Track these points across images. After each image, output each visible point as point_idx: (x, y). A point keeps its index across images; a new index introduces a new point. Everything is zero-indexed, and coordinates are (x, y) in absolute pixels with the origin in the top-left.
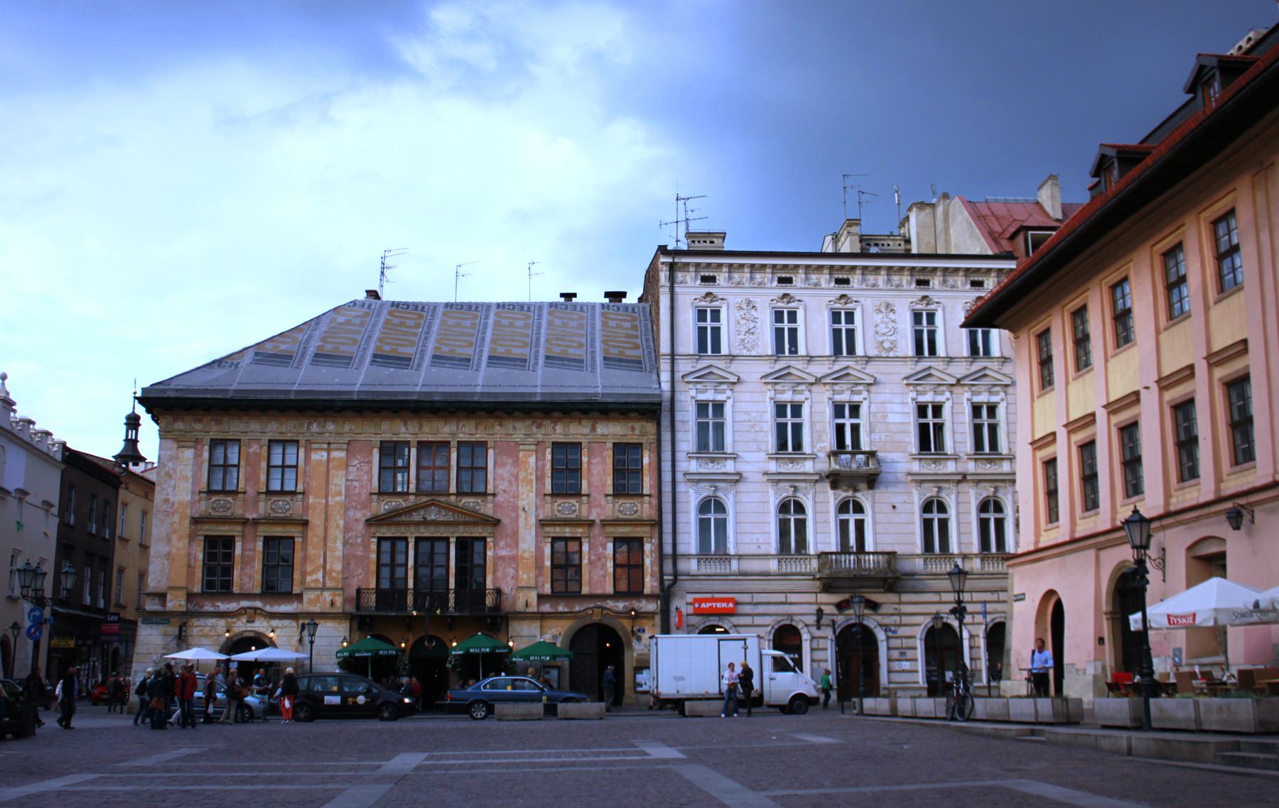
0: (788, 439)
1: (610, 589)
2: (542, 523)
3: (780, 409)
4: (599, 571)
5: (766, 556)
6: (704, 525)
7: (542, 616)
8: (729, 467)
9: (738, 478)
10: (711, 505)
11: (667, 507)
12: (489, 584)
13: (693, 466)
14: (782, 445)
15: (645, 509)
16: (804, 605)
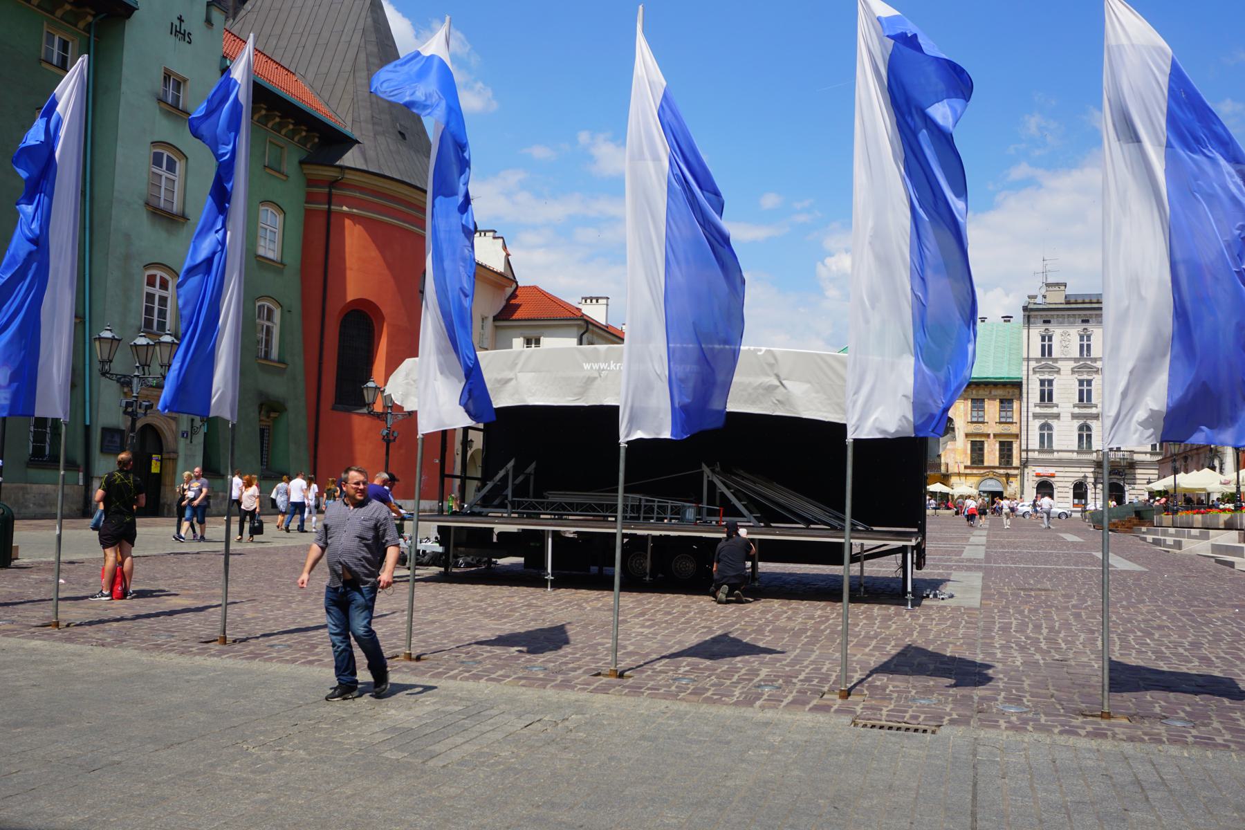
0: (1084, 397)
1: (997, 464)
2: (967, 435)
3: (1081, 382)
4: (992, 455)
5: (1073, 451)
6: (1042, 436)
7: (966, 475)
8: (1055, 410)
9: (1057, 416)
10: (1046, 427)
11: (1024, 428)
12: (943, 460)
13: (1038, 410)
14: (1081, 400)
15: (1014, 429)
16: (1089, 472)
